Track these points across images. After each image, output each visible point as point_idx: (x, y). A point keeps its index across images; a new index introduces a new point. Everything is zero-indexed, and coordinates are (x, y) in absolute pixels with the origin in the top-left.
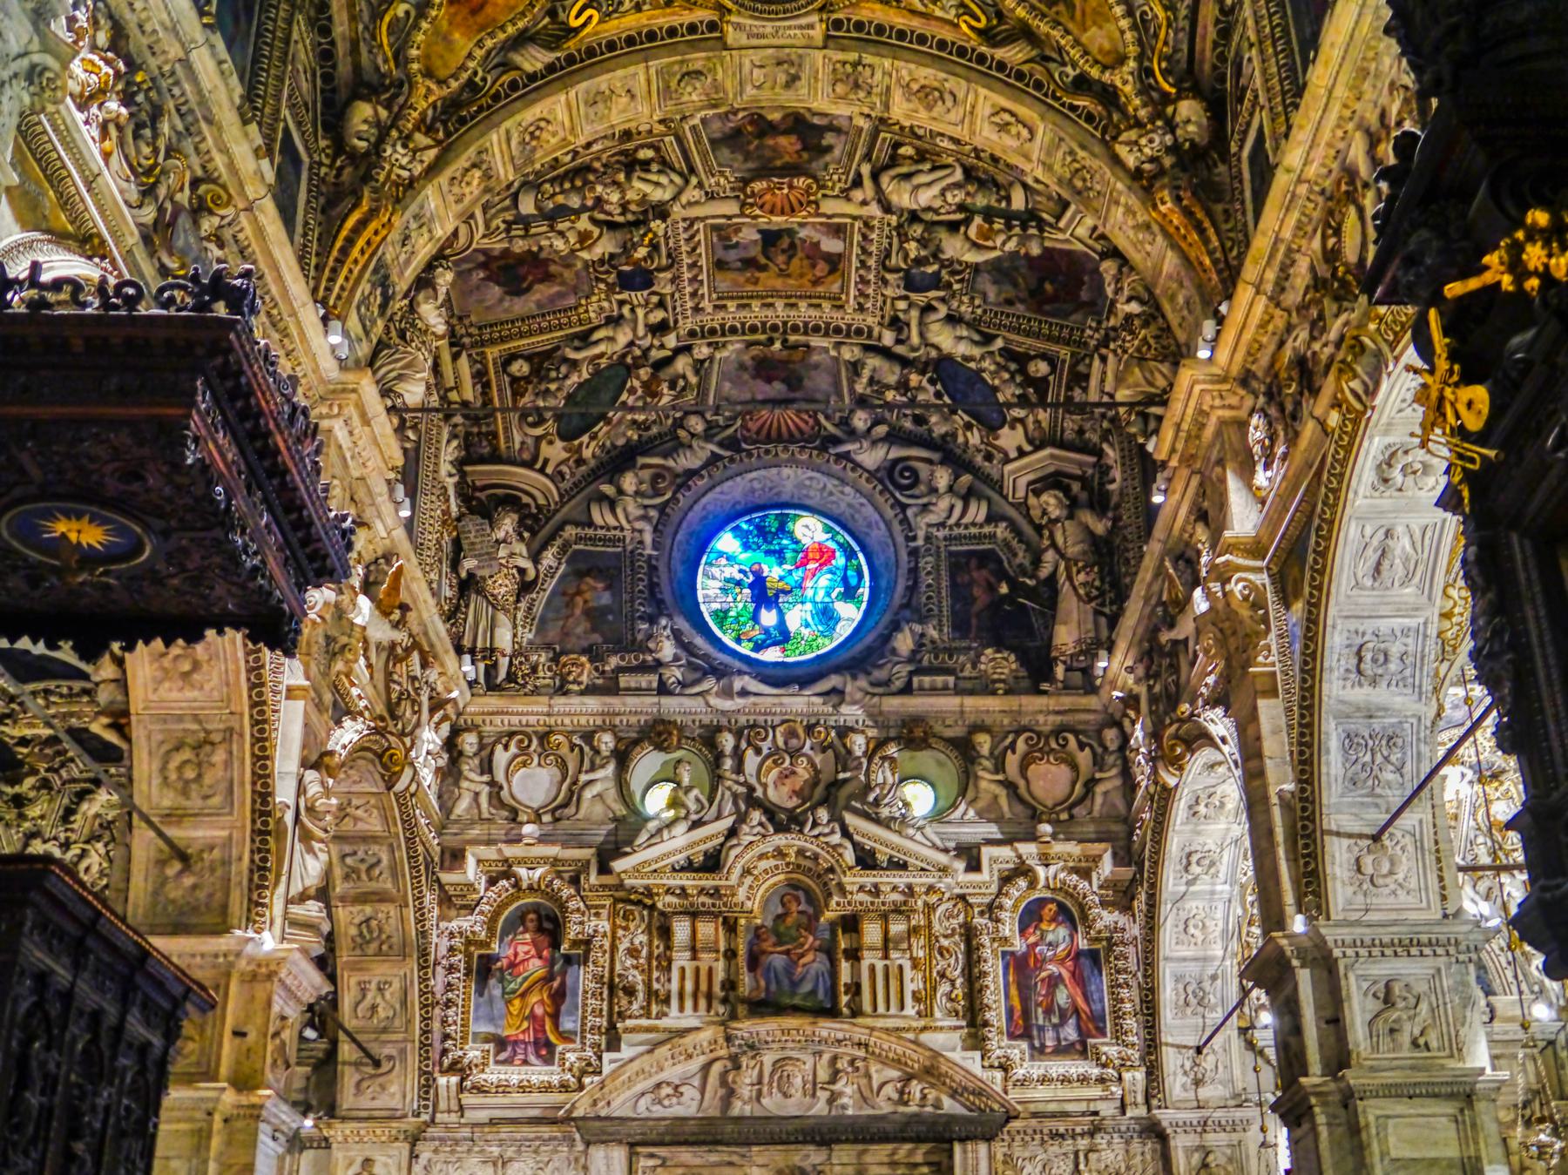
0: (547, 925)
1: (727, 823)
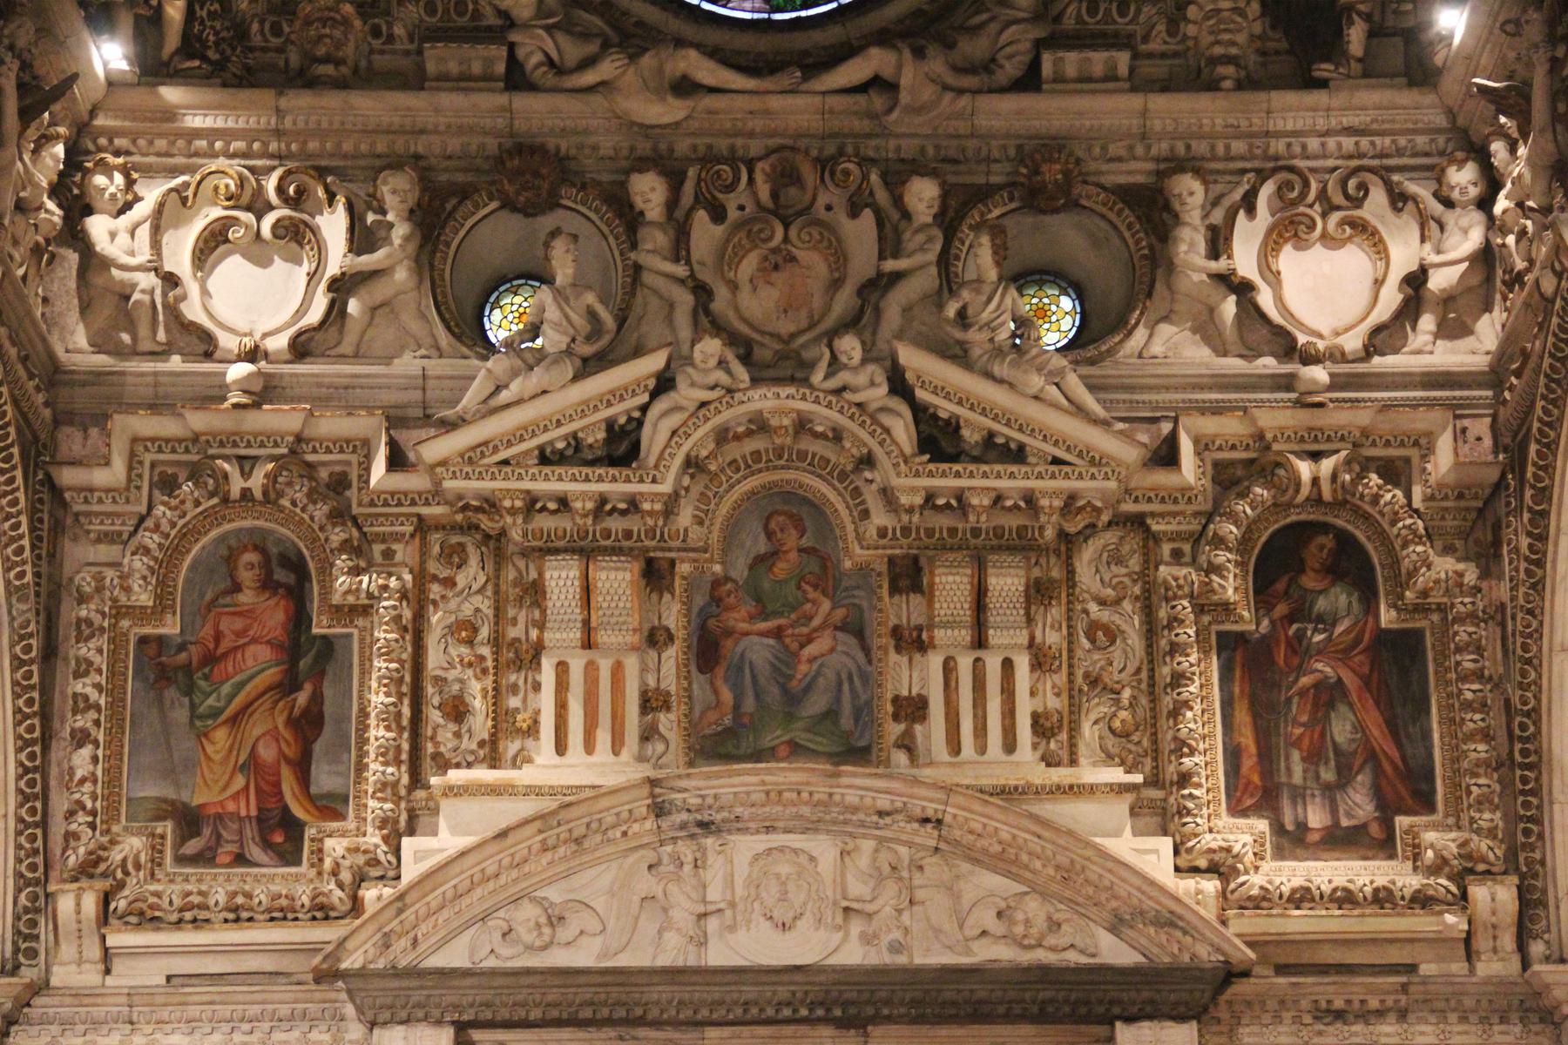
0: (280, 575)
1: (653, 363)
